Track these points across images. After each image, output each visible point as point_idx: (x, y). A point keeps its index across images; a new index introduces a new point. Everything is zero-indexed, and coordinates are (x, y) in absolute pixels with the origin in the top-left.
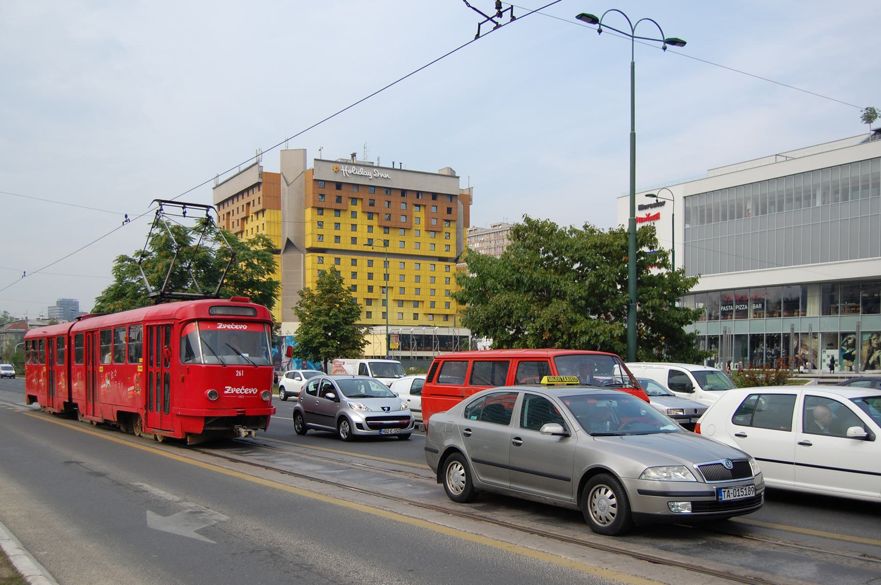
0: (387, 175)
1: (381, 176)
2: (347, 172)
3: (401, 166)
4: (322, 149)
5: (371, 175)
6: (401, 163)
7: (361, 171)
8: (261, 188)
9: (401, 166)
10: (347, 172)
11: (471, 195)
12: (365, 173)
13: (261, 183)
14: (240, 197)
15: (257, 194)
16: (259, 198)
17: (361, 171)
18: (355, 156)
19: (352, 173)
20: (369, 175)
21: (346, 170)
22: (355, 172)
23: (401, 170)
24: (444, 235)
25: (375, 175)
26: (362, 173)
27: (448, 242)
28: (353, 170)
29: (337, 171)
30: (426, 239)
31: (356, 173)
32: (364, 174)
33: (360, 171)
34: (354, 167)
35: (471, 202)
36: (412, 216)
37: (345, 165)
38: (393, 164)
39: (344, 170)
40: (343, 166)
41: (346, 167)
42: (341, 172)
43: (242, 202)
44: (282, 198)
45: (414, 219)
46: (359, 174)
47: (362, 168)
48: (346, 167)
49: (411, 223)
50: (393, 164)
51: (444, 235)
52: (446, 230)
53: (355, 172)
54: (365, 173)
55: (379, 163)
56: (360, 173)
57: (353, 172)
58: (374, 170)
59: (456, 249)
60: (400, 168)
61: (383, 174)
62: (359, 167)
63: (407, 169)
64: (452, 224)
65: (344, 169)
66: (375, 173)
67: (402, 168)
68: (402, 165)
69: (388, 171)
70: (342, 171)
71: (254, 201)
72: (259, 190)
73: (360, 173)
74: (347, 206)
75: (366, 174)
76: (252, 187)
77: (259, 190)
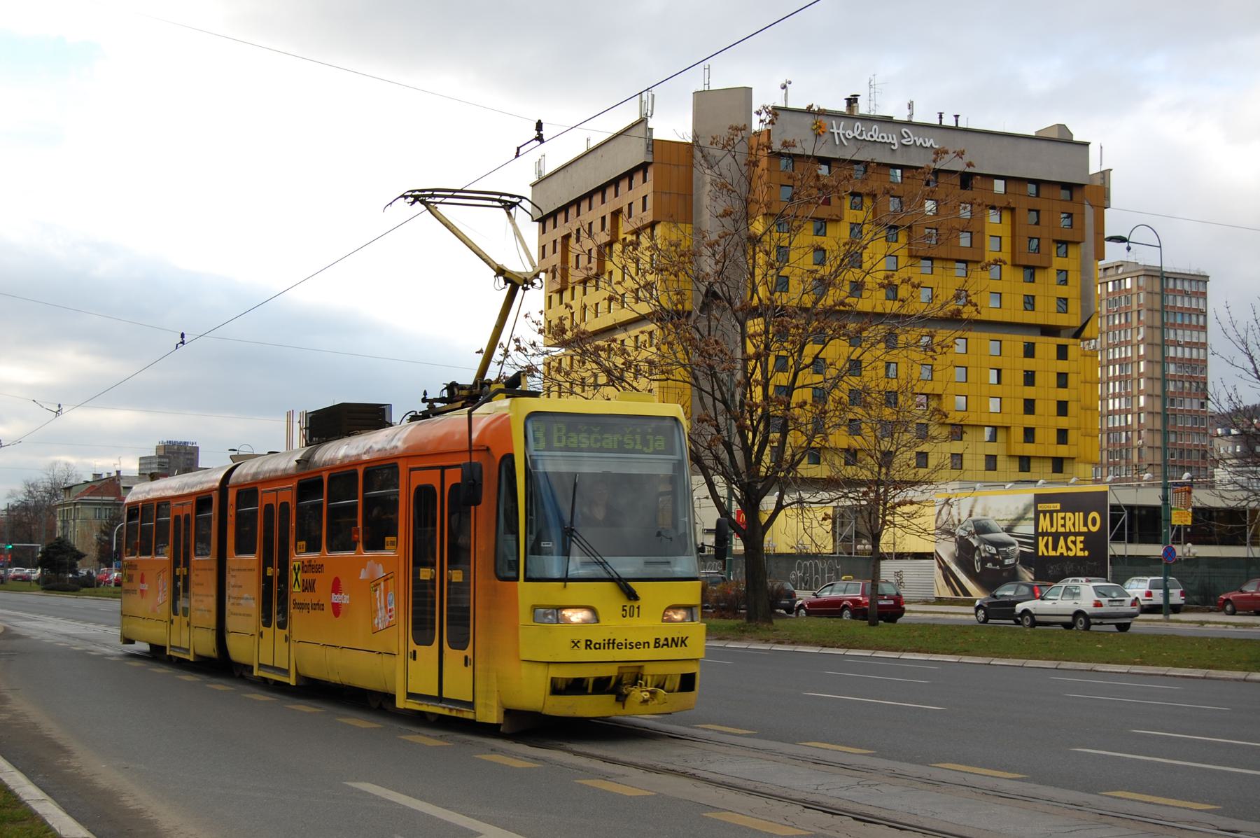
0: (932, 141)
1: (918, 144)
2: (844, 135)
3: (957, 121)
4: (788, 85)
5: (895, 141)
6: (957, 116)
7: (875, 133)
8: (650, 175)
9: (957, 121)
10: (844, 135)
11: (1107, 186)
12: (883, 137)
13: (651, 163)
14: (597, 199)
15: (644, 188)
16: (644, 198)
17: (875, 133)
18: (856, 101)
19: (854, 137)
20: (890, 140)
21: (841, 132)
22: (861, 134)
23: (956, 129)
24: (1052, 275)
25: (904, 141)
26: (875, 138)
27: (1063, 291)
28: (856, 131)
29: (818, 132)
30: (1013, 283)
31: (864, 137)
32: (880, 140)
33: (873, 133)
34: (858, 124)
35: (1106, 203)
36: (983, 233)
37: (837, 119)
38: (941, 117)
39: (835, 131)
40: (834, 122)
41: (842, 123)
42: (830, 135)
43: (603, 208)
44: (694, 197)
45: (987, 237)
46: (869, 138)
47: (875, 127)
48: (842, 123)
49: (982, 248)
50: (941, 117)
51: (1052, 275)
52: (1058, 263)
53: (861, 134)
54: (883, 137)
55: (911, 115)
56: (872, 136)
57: (856, 134)
58: (903, 130)
59: (1082, 306)
60: (954, 124)
61: (921, 140)
62: (869, 123)
63: (971, 126)
64: (1072, 251)
65: (838, 129)
66: (904, 138)
67: (960, 125)
68: (960, 118)
69: (931, 131)
70: (833, 133)
71: (630, 205)
72: (645, 181)
73: (872, 136)
74: (842, 211)
75: (886, 140)
76: (629, 175)
77: (645, 181)
